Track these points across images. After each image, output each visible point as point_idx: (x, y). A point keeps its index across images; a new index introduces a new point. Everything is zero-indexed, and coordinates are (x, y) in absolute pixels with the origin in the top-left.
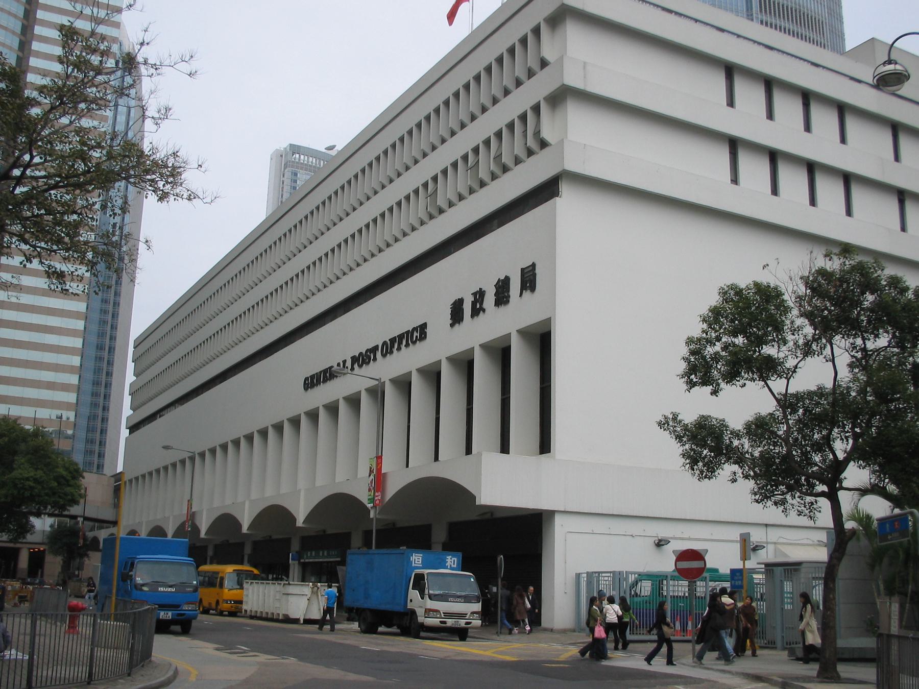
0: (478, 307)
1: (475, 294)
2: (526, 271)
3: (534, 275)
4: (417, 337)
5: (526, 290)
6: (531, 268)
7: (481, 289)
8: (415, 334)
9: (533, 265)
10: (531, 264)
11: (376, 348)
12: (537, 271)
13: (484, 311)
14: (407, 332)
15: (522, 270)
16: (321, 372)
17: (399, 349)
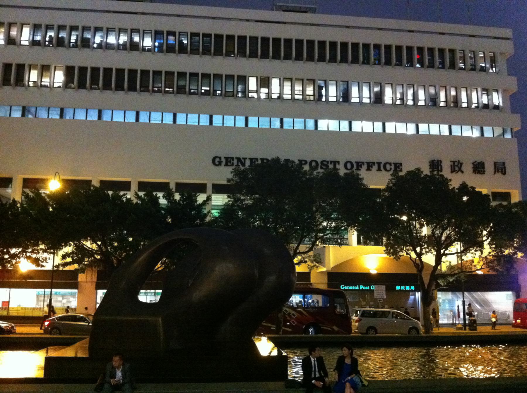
0: (457, 169)
1: (454, 162)
2: (497, 164)
3: (505, 168)
4: (391, 169)
5: (498, 172)
6: (502, 164)
7: (459, 161)
8: (388, 167)
9: (504, 163)
10: (502, 161)
11: (338, 162)
12: (507, 165)
13: (462, 172)
14: (379, 164)
15: (495, 163)
16: (245, 159)
17: (369, 169)
